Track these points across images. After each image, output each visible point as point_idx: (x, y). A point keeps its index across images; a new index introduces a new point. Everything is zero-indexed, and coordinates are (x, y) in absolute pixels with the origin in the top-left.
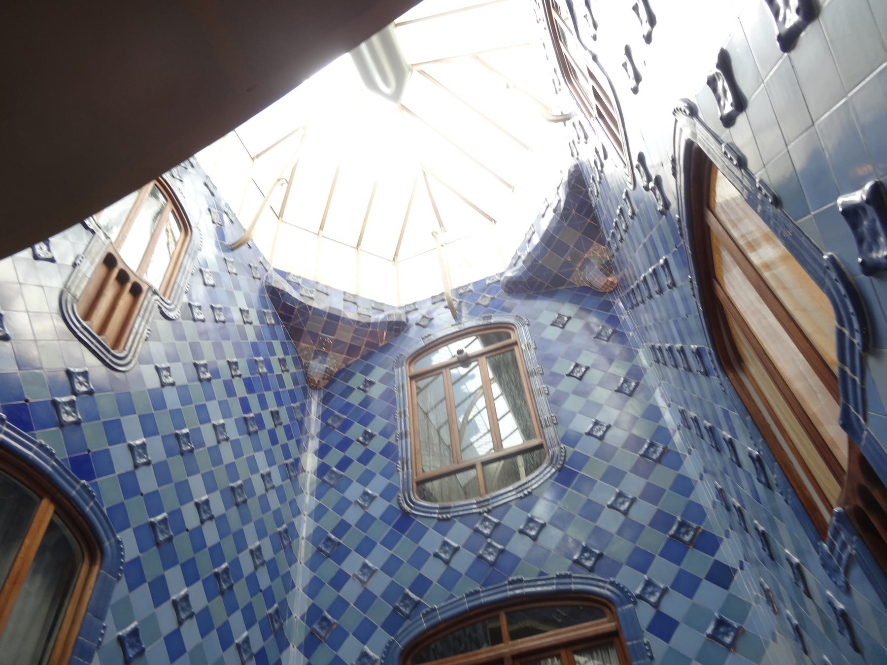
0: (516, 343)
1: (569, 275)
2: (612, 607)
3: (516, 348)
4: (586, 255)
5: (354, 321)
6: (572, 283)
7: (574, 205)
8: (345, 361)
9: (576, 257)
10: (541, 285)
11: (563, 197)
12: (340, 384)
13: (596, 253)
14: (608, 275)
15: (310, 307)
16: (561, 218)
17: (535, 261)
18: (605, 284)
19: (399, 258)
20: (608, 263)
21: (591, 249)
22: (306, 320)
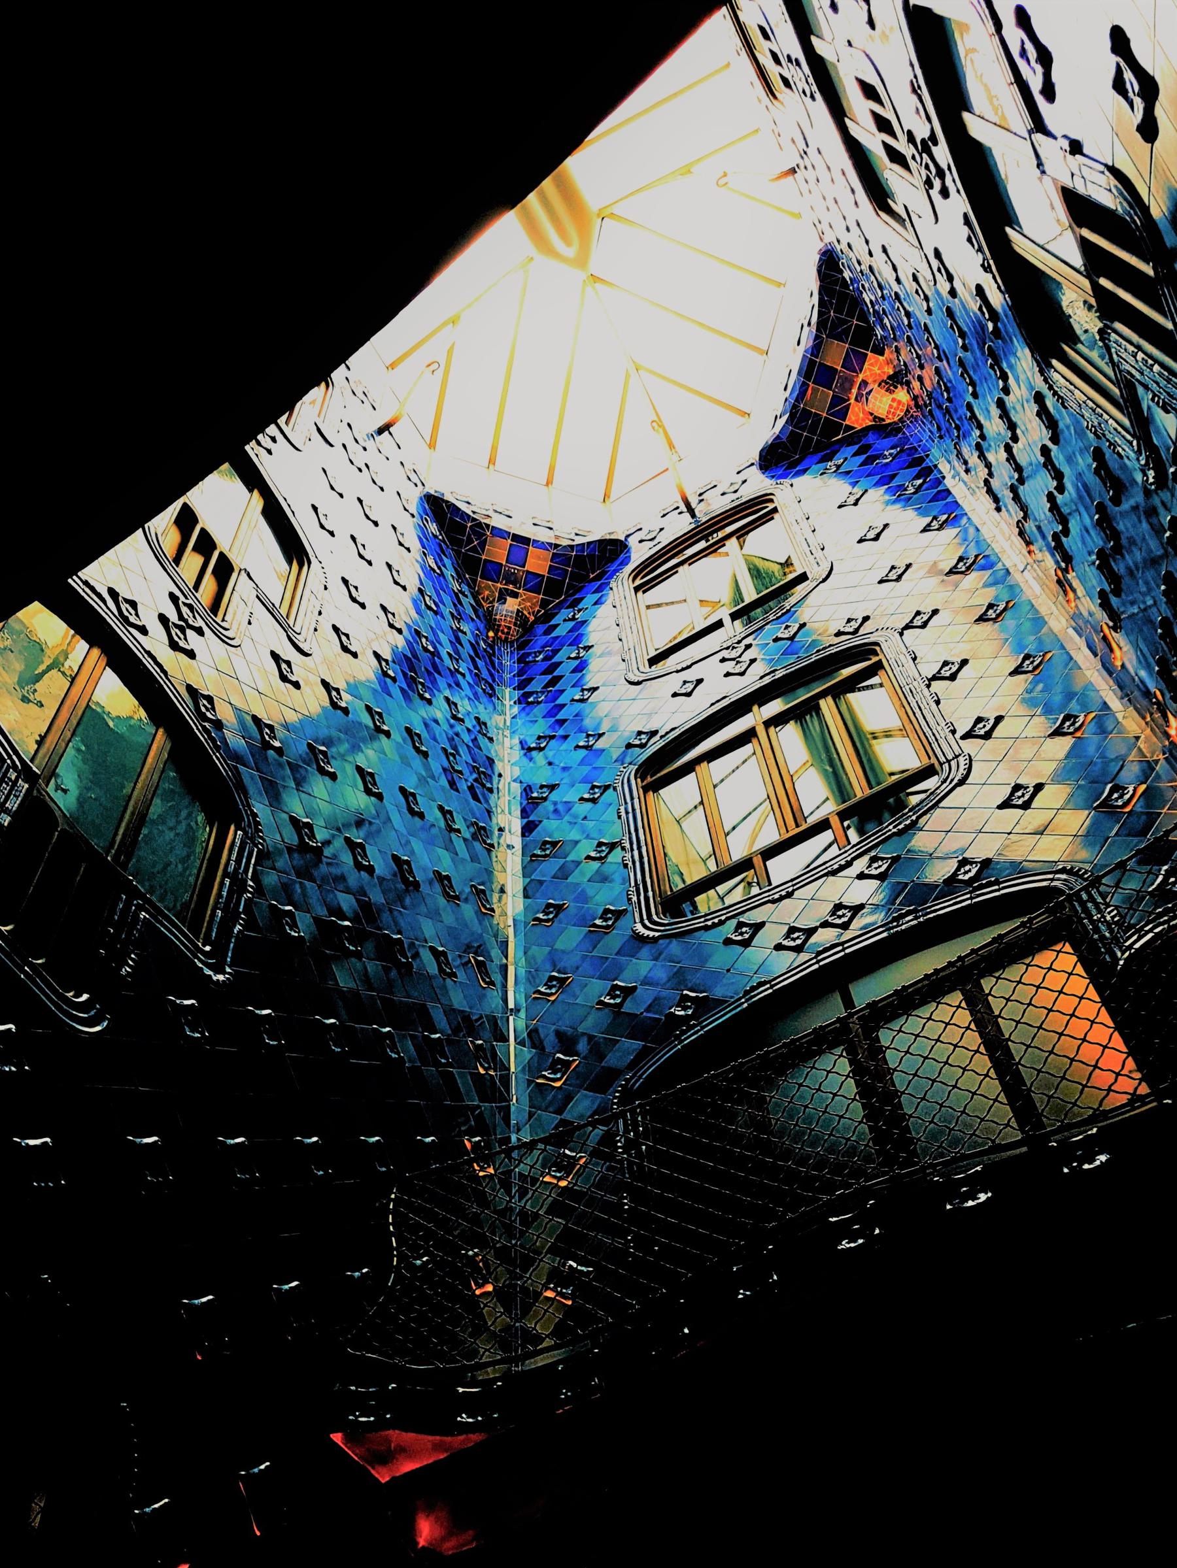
0: (775, 510)
1: (844, 414)
2: (877, 648)
3: (776, 516)
4: (861, 376)
5: (550, 544)
6: (849, 428)
7: (831, 304)
8: (544, 604)
9: (847, 384)
10: (809, 440)
11: (816, 299)
12: (541, 628)
13: (876, 367)
14: (891, 392)
15: (488, 526)
16: (818, 330)
17: (794, 406)
18: (891, 406)
19: (613, 496)
20: (890, 377)
21: (866, 366)
22: (483, 544)
